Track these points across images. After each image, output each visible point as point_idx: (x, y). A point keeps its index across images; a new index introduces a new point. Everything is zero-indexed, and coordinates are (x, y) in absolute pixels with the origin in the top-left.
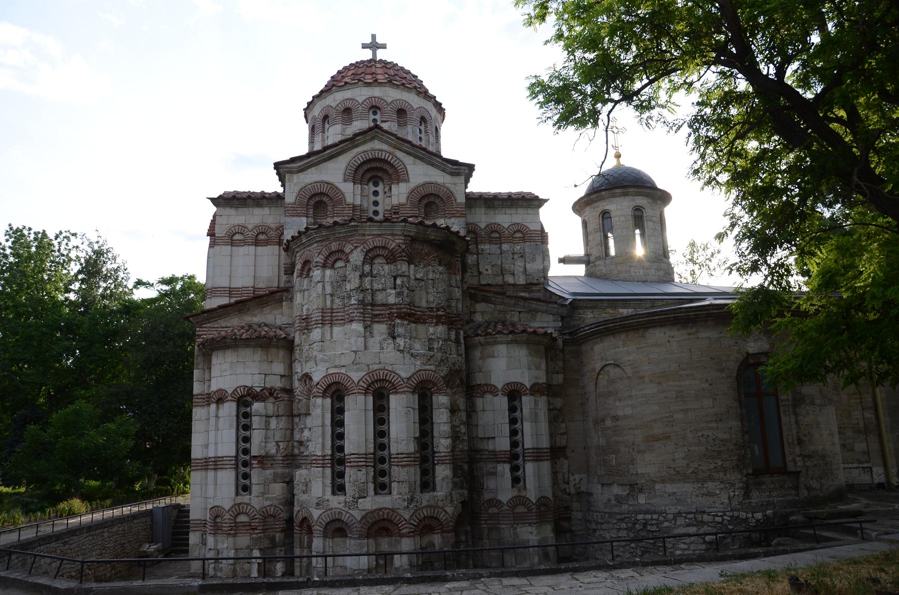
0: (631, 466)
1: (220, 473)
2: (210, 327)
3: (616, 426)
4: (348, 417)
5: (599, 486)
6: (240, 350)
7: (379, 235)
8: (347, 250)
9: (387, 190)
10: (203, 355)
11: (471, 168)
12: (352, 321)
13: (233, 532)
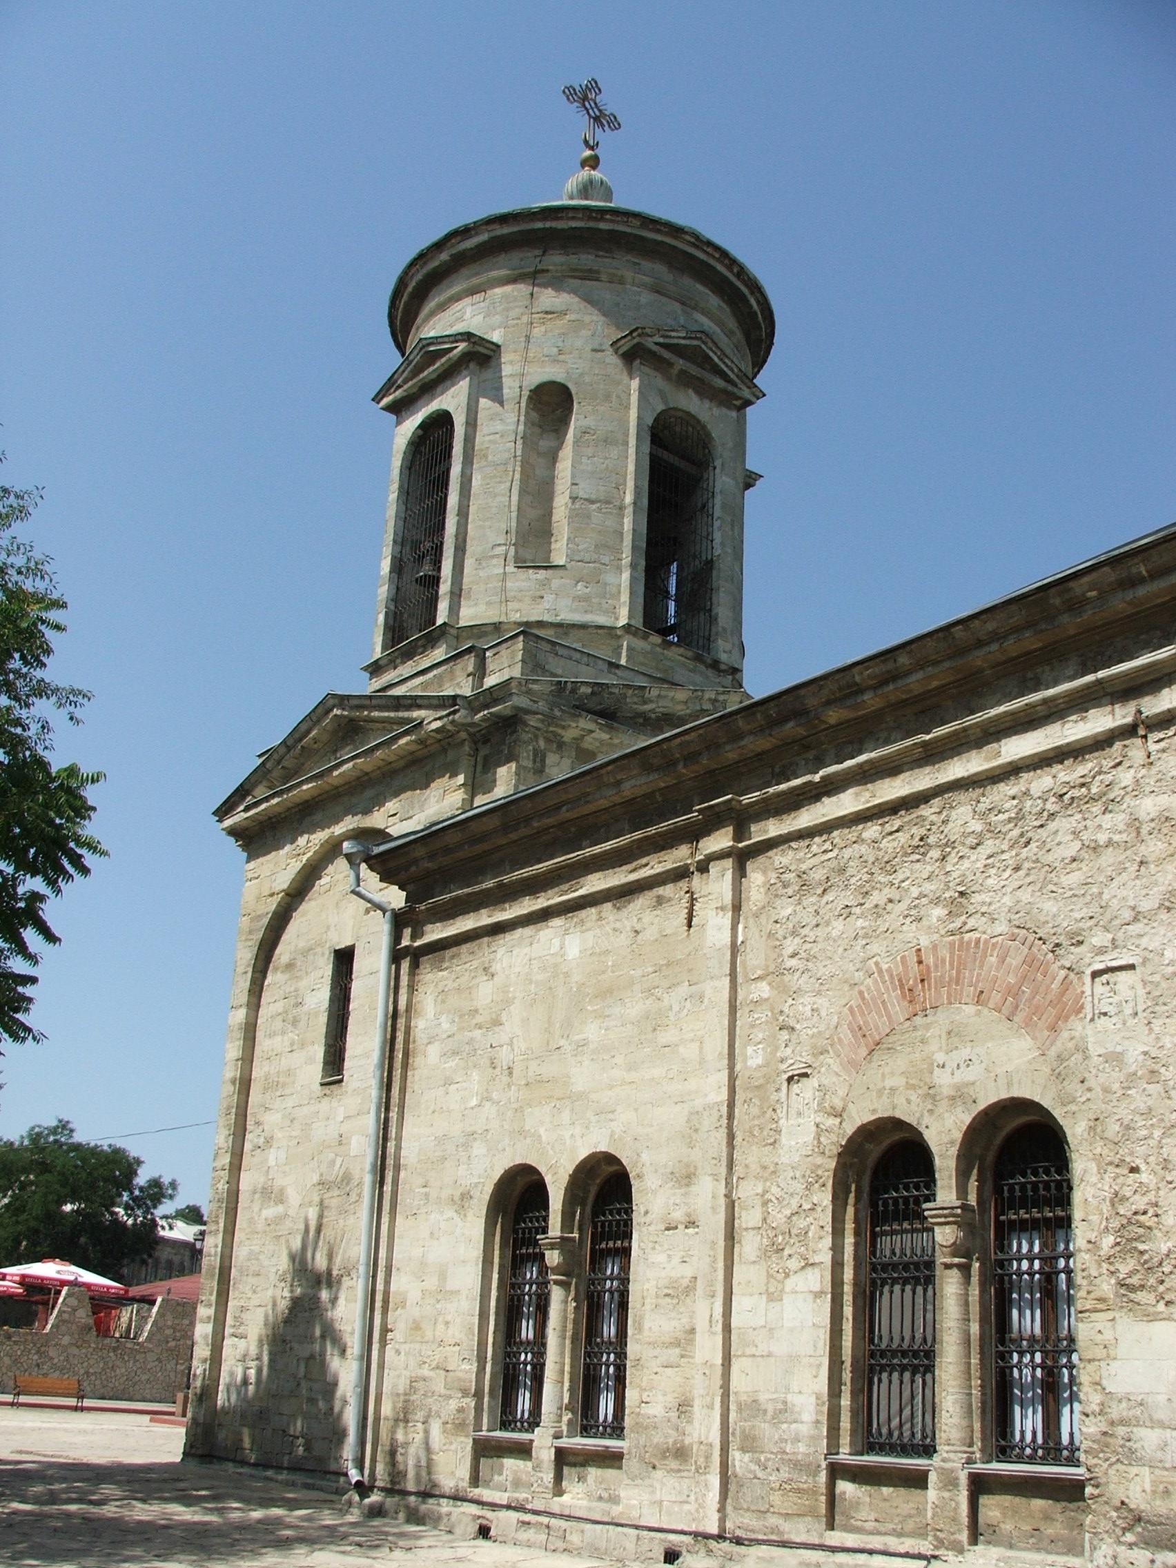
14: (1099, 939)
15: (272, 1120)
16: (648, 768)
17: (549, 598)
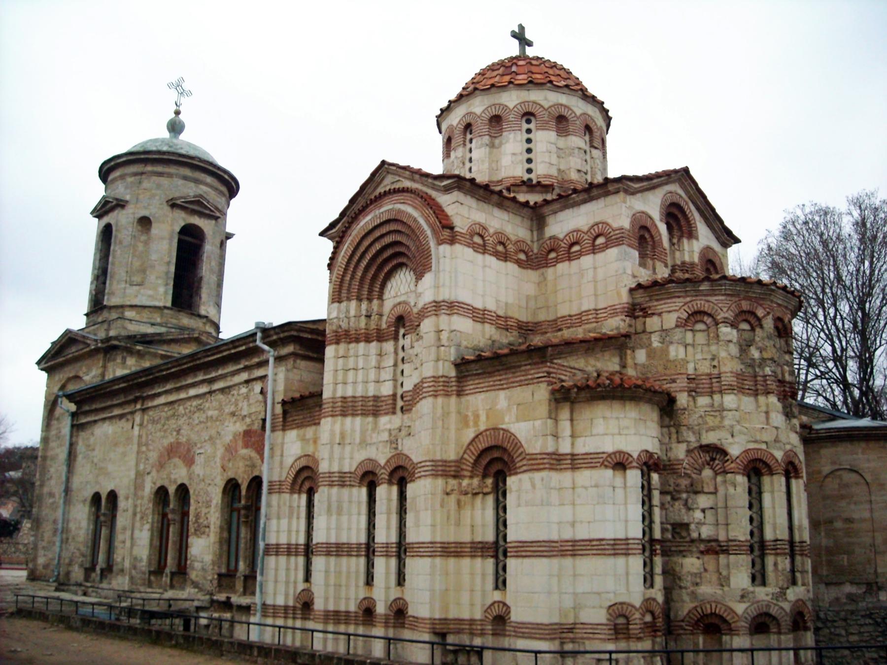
0: (868, 566)
1: (631, 559)
2: (560, 365)
3: (849, 528)
4: (767, 498)
5: (824, 585)
6: (641, 403)
7: (779, 305)
8: (760, 313)
9: (675, 241)
10: (556, 400)
11: (737, 241)
12: (769, 393)
13: (642, 635)
14: (199, 445)
15: (52, 470)
16: (124, 382)
17: (140, 296)
